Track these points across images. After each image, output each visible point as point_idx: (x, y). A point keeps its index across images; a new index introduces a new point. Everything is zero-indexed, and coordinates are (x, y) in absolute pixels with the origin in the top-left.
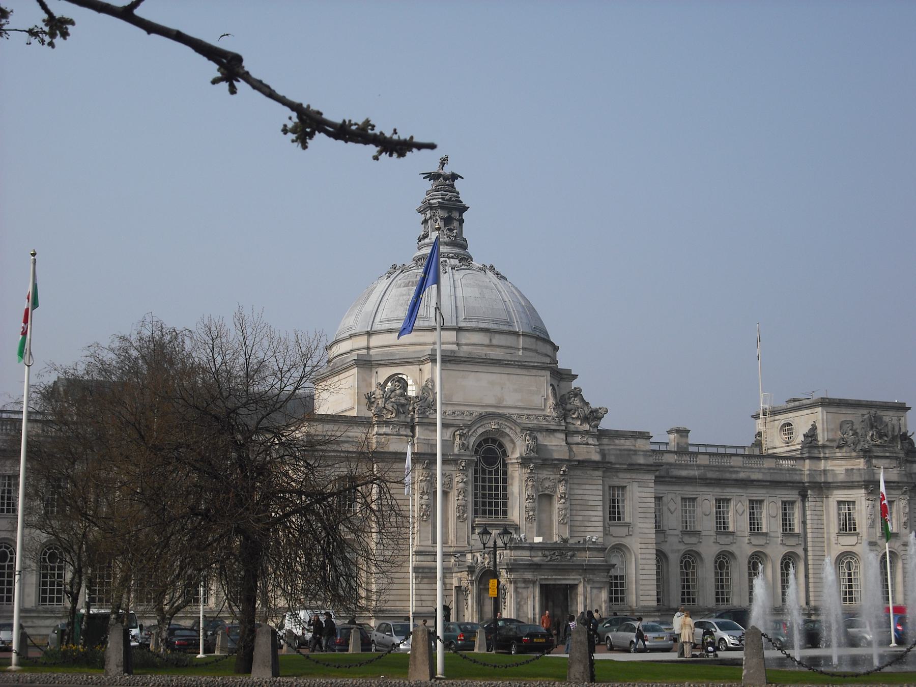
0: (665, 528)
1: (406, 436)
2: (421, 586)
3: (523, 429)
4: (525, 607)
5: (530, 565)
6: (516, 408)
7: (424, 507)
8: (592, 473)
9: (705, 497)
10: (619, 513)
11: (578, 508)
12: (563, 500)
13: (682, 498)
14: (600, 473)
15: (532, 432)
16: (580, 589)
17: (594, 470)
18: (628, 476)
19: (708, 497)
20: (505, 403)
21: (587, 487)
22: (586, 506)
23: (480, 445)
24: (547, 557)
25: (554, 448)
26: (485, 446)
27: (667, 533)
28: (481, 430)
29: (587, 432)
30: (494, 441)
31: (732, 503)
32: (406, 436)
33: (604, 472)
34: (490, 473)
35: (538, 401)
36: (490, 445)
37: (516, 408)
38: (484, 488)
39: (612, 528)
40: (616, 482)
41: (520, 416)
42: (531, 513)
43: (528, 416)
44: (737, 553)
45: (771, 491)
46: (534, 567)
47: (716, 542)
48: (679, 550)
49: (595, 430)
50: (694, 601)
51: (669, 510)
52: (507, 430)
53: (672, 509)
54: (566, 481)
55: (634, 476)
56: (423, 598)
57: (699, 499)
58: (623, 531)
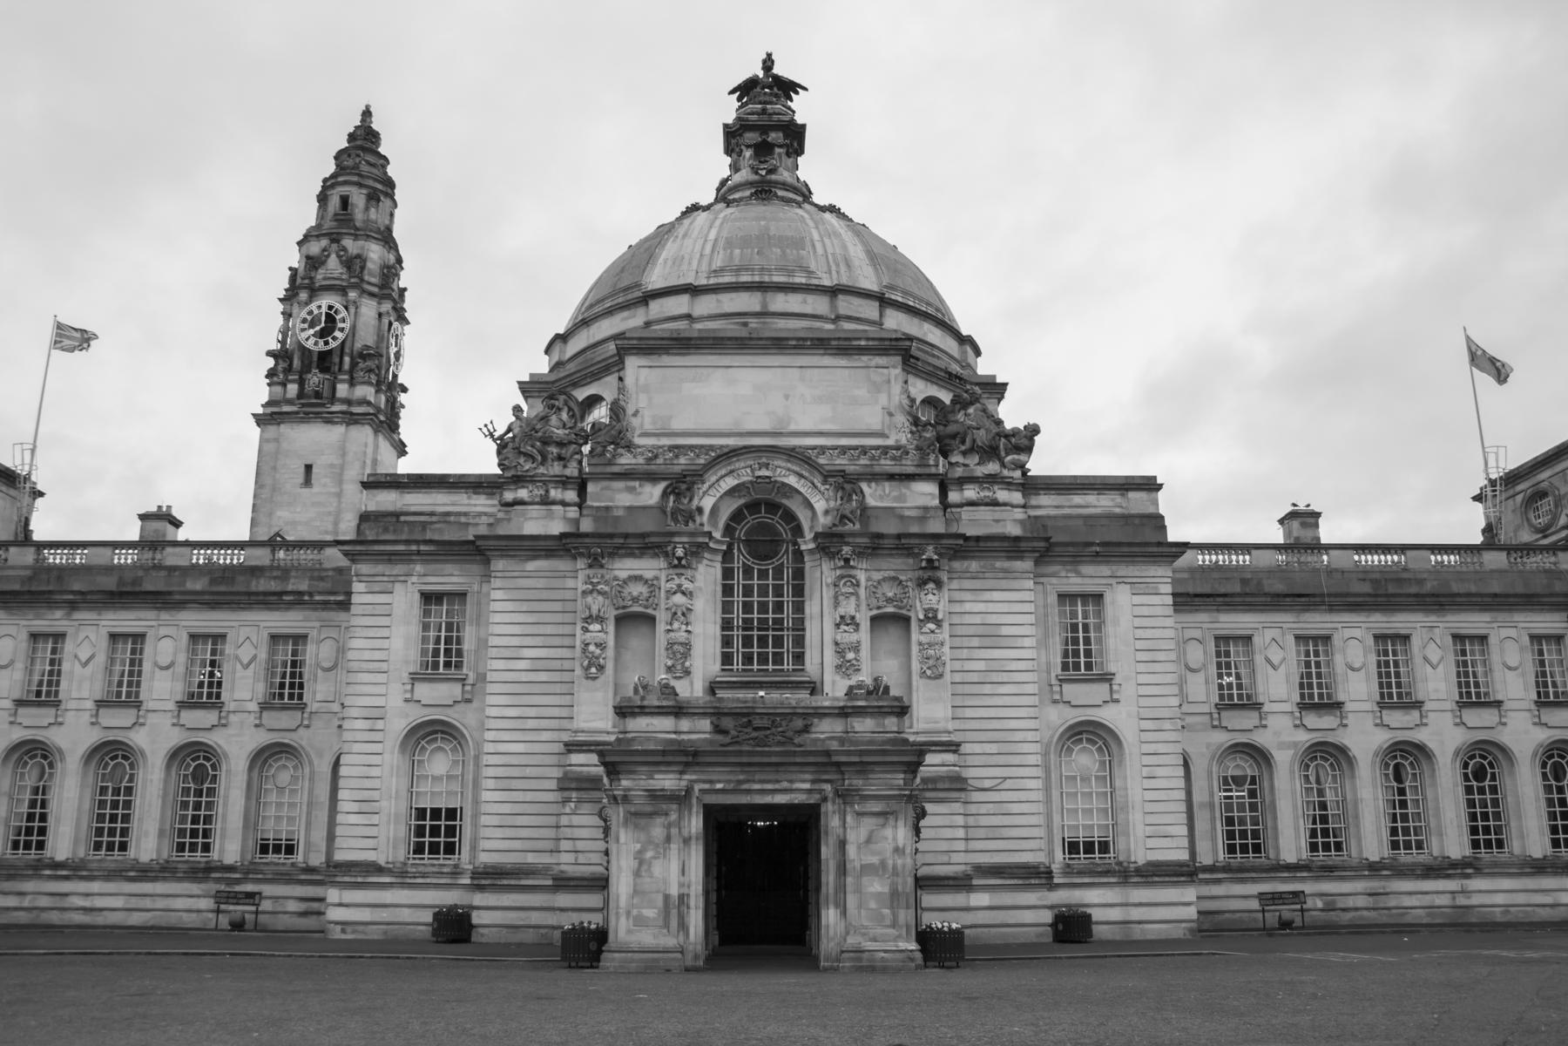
0: (1261, 700)
1: (564, 504)
2: (576, 820)
3: (827, 476)
4: (657, 869)
5: (664, 753)
7: (592, 648)
8: (1007, 564)
9: (1348, 633)
10: (1088, 653)
11: (975, 642)
12: (932, 626)
13: (1298, 638)
14: (1027, 565)
15: (845, 483)
16: (831, 821)
17: (1009, 558)
18: (1105, 570)
19: (1357, 633)
20: (793, 427)
21: (996, 595)
22: (991, 636)
23: (737, 517)
24: (725, 732)
25: (907, 513)
26: (750, 520)
27: (1266, 708)
28: (730, 482)
29: (992, 479)
30: (773, 507)
31: (1416, 642)
32: (564, 504)
33: (1037, 563)
34: (763, 574)
35: (871, 417)
36: (763, 517)
38: (747, 607)
39: (1066, 687)
40: (1074, 582)
41: (823, 450)
42: (850, 656)
43: (844, 450)
44: (1432, 745)
45: (1502, 616)
46: (684, 757)
47: (1382, 725)
48: (1295, 744)
49: (1018, 474)
50: (1338, 846)
51: (1268, 660)
52: (792, 480)
53: (1276, 660)
54: (939, 584)
55: (1123, 570)
56: (580, 845)
57: (1337, 640)
58: (1099, 691)
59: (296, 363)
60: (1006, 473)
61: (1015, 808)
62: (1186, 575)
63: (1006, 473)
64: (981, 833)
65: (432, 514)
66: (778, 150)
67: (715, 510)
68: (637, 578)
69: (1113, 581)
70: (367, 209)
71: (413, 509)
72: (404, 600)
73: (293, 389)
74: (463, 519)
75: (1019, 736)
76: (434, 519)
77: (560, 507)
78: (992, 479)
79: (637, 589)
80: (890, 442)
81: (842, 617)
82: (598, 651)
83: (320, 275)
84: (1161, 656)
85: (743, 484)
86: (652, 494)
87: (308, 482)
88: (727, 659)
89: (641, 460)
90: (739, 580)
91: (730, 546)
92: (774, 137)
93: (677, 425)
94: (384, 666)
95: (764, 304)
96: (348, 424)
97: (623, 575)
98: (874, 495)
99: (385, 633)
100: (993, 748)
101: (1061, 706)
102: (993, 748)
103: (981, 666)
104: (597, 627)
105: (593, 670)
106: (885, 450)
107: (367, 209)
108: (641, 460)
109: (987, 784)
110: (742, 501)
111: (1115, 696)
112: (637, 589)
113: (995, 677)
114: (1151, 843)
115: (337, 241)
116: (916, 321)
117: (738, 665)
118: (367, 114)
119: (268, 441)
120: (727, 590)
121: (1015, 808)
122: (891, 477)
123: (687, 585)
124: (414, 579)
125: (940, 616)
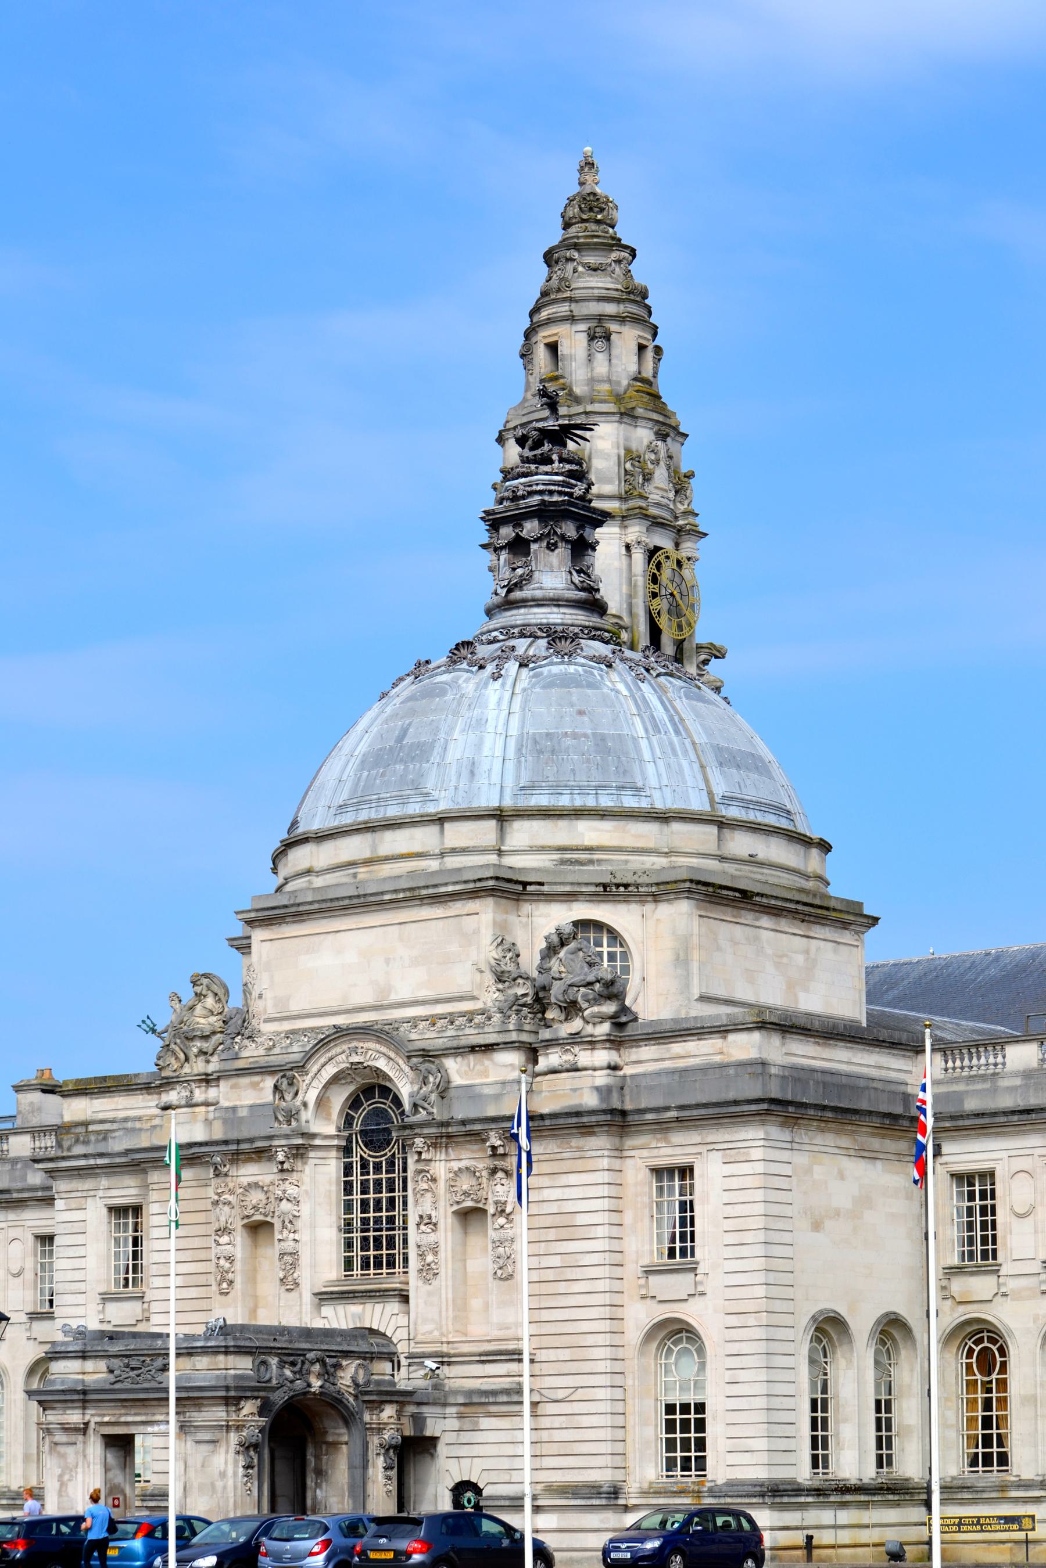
6: (416, 1003)
11: (552, 1234)
12: (502, 1221)
20: (394, 997)
21: (573, 1179)
25: (487, 1091)
26: (366, 1107)
28: (330, 1071)
29: (575, 1039)
34: (378, 1168)
36: (378, 1102)
37: (416, 1003)
41: (414, 1022)
43: (432, 1020)
52: (381, 1064)
60: (589, 1029)
61: (585, 1421)
62: (1018, 1082)
63: (589, 1029)
64: (554, 1449)
65: (113, 1121)
66: (534, 547)
67: (321, 1102)
68: (256, 1185)
69: (703, 1149)
70: (590, 358)
71: (101, 1116)
72: (94, 1215)
74: (129, 1125)
75: (590, 1340)
76: (115, 1126)
77: (203, 1109)
78: (575, 1039)
79: (256, 1197)
80: (478, 1005)
81: (421, 1217)
82: (227, 1265)
84: (749, 1237)
85: (341, 1071)
86: (265, 1089)
88: (348, 1264)
89: (261, 1052)
90: (357, 1178)
91: (349, 1140)
92: (531, 528)
93: (296, 1006)
94: (81, 1287)
95: (374, 847)
97: (245, 1181)
98: (457, 1070)
99: (81, 1251)
100: (565, 1354)
101: (648, 1301)
102: (565, 1354)
103: (555, 1261)
104: (225, 1239)
105: (225, 1285)
106: (470, 1016)
107: (590, 358)
108: (262, 1052)
109: (560, 1394)
110: (351, 1088)
111: (700, 1288)
112: (256, 1197)
113: (570, 1274)
114: (732, 1459)
116: (562, 824)
117: (357, 1272)
120: (348, 1188)
121: (585, 1421)
122: (473, 1049)
123: (292, 1191)
124: (101, 1193)
125: (508, 1210)
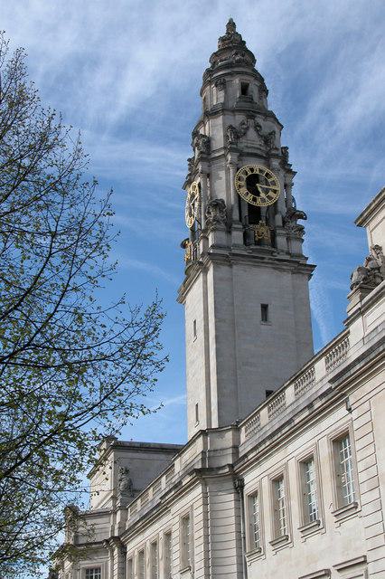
59: (236, 216)
73: (237, 236)
83: (243, 144)
87: (265, 317)
96: (293, 273)
115: (252, 117)
118: (231, 25)
119: (221, 279)
